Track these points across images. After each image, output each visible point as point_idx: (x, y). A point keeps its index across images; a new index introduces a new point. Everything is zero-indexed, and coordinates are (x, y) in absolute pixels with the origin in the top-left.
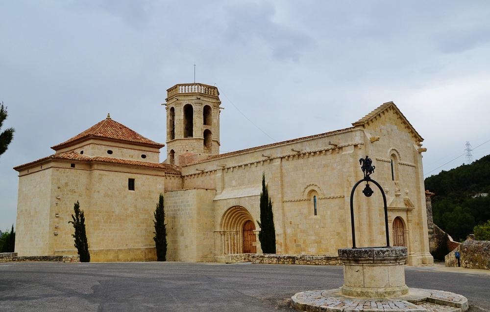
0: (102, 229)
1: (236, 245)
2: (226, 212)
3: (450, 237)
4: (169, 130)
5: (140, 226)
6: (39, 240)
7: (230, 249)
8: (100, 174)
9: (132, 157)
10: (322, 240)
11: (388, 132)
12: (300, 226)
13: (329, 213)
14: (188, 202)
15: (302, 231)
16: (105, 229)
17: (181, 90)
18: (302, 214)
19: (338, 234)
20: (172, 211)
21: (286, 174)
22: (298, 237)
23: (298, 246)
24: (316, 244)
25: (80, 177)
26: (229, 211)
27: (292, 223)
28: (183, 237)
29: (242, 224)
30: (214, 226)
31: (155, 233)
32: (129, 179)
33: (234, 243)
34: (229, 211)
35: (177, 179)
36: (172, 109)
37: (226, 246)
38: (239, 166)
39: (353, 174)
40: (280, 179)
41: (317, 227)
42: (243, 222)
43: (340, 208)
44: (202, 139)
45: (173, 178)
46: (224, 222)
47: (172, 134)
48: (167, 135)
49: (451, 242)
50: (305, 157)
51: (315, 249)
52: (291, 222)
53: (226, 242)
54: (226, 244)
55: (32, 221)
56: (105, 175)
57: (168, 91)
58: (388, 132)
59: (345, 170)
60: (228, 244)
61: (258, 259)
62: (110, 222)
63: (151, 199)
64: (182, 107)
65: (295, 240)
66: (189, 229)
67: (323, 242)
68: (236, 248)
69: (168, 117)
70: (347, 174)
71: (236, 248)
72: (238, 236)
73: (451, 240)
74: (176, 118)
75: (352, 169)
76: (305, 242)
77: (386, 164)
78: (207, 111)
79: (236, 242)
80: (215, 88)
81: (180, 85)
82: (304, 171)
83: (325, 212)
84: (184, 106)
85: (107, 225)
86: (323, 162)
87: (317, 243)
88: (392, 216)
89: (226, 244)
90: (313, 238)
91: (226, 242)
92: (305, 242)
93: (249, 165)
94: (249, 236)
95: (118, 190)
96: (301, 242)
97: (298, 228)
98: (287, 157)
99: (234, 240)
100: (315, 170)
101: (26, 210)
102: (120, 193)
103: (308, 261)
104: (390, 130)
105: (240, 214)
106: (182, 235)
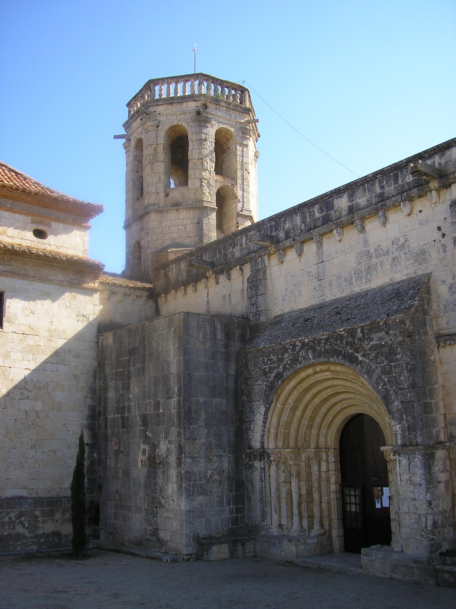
7: (296, 511)
17: (161, 91)
33: (310, 493)
36: (140, 143)
37: (284, 501)
44: (213, 209)
53: (284, 491)
54: (284, 495)
57: (128, 105)
60: (290, 493)
68: (316, 509)
71: (316, 509)
72: (324, 468)
78: (223, 148)
80: (243, 90)
84: (166, 127)
89: (284, 495)
105: (330, 392)
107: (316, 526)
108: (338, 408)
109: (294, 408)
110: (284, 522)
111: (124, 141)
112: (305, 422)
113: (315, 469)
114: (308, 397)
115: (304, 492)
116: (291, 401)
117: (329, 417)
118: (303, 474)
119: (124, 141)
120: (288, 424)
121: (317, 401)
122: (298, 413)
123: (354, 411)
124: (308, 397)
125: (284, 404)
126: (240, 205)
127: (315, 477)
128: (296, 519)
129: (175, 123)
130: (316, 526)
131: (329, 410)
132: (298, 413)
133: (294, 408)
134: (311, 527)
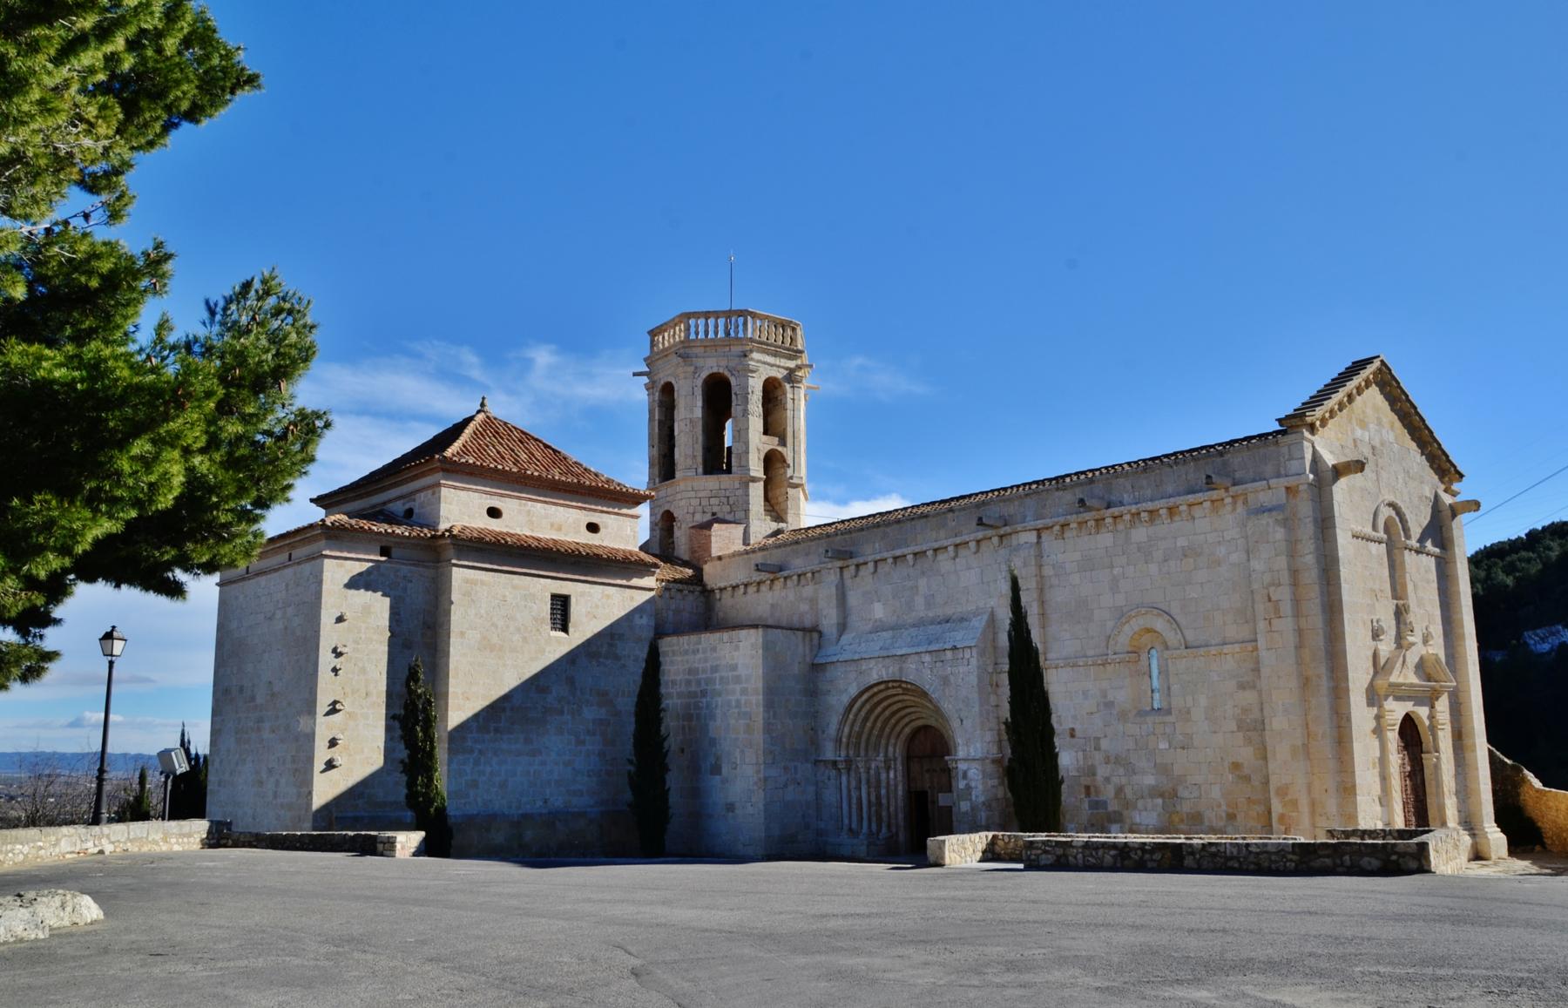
0: (472, 751)
1: (884, 801)
2: (855, 700)
3: (1530, 776)
4: (655, 451)
5: (583, 743)
6: (283, 781)
8: (467, 581)
9: (559, 529)
10: (1180, 789)
11: (1373, 448)
12: (1104, 744)
13: (1203, 701)
14: (734, 668)
15: (1117, 760)
16: (480, 752)
18: (1109, 705)
19: (1236, 766)
20: (680, 695)
21: (1055, 581)
22: (1099, 778)
23: (1096, 805)
24: (1160, 801)
25: (405, 589)
26: (865, 697)
27: (1077, 733)
28: (718, 777)
29: (903, 737)
30: (814, 742)
31: (630, 762)
32: (554, 597)
33: (878, 797)
34: (865, 697)
35: (691, 597)
36: (668, 389)
38: (895, 558)
39: (1285, 577)
40: (1035, 595)
41: (1163, 745)
42: (907, 730)
43: (1242, 687)
45: (679, 596)
46: (846, 730)
47: (665, 467)
48: (651, 466)
49: (1538, 791)
50: (1121, 527)
51: (1155, 815)
52: (1073, 730)
53: (854, 794)
54: (854, 801)
55: (260, 720)
56: (483, 583)
58: (1373, 448)
59: (1257, 565)
60: (860, 799)
61: (1046, 852)
62: (497, 730)
63: (617, 658)
64: (700, 382)
65: (1087, 788)
66: (737, 754)
67: (1182, 792)
69: (651, 412)
70: (1267, 578)
71: (884, 814)
72: (892, 775)
73: (1537, 784)
74: (681, 414)
75: (1282, 562)
76: (1120, 790)
77: (1373, 547)
79: (883, 792)
81: (696, 315)
82: (1116, 571)
83: (1189, 699)
84: (704, 375)
85: (487, 737)
86: (1182, 542)
87: (1162, 795)
88: (1396, 711)
90: (1150, 780)
91: (854, 794)
92: (1120, 790)
93: (930, 553)
94: (927, 776)
95: (518, 630)
96: (1108, 793)
97: (1097, 748)
98: (1057, 528)
99: (878, 787)
100: (1153, 568)
101: (241, 689)
102: (525, 639)
103: (1232, 858)
104: (1376, 443)
105: (900, 705)
106: (716, 770)
107: (884, 830)
108: (907, 720)
109: (866, 719)
110: (854, 826)
111: (645, 380)
112: (875, 732)
113: (883, 776)
114: (879, 709)
115: (873, 798)
116: (863, 713)
117: (898, 729)
118: (873, 780)
119: (645, 380)
120: (860, 735)
121: (887, 713)
122: (869, 724)
123: (920, 723)
124: (879, 709)
125: (856, 715)
126: (789, 472)
127: (884, 784)
128: (865, 824)
129: (715, 370)
130: (884, 830)
131: (898, 722)
132: (869, 724)
133: (866, 719)
134: (879, 830)
